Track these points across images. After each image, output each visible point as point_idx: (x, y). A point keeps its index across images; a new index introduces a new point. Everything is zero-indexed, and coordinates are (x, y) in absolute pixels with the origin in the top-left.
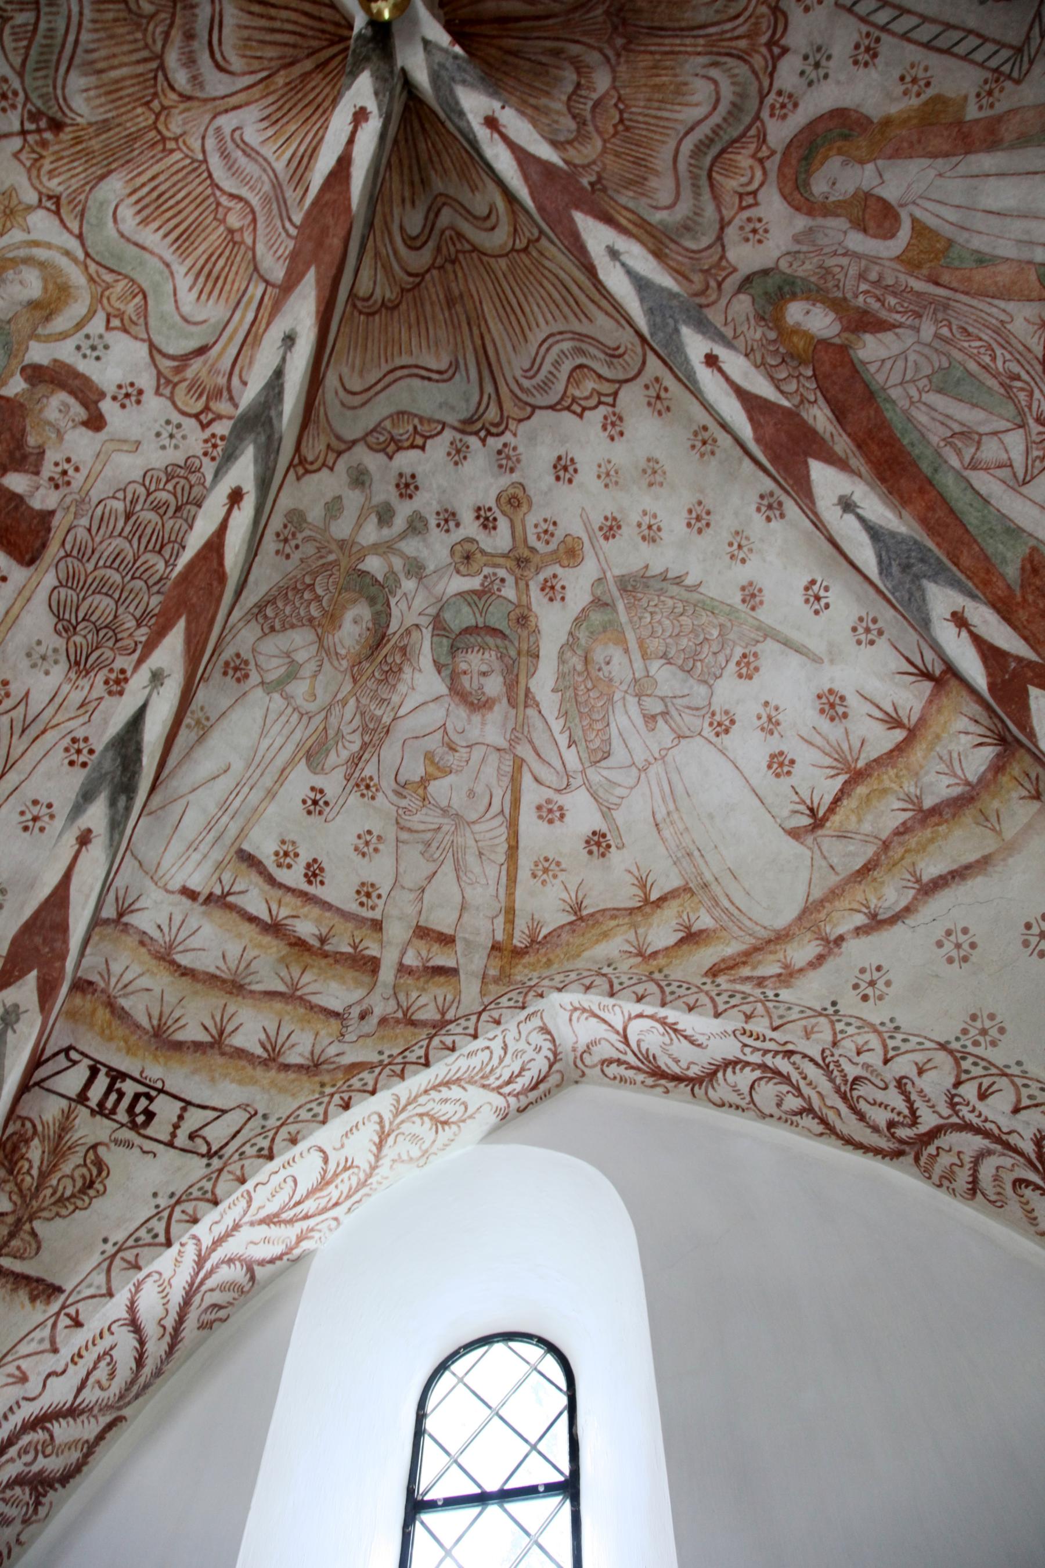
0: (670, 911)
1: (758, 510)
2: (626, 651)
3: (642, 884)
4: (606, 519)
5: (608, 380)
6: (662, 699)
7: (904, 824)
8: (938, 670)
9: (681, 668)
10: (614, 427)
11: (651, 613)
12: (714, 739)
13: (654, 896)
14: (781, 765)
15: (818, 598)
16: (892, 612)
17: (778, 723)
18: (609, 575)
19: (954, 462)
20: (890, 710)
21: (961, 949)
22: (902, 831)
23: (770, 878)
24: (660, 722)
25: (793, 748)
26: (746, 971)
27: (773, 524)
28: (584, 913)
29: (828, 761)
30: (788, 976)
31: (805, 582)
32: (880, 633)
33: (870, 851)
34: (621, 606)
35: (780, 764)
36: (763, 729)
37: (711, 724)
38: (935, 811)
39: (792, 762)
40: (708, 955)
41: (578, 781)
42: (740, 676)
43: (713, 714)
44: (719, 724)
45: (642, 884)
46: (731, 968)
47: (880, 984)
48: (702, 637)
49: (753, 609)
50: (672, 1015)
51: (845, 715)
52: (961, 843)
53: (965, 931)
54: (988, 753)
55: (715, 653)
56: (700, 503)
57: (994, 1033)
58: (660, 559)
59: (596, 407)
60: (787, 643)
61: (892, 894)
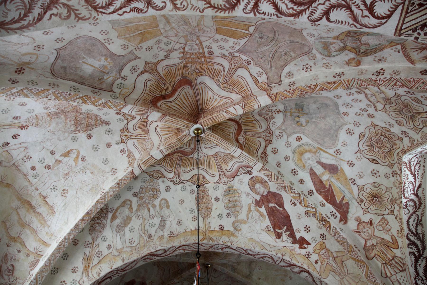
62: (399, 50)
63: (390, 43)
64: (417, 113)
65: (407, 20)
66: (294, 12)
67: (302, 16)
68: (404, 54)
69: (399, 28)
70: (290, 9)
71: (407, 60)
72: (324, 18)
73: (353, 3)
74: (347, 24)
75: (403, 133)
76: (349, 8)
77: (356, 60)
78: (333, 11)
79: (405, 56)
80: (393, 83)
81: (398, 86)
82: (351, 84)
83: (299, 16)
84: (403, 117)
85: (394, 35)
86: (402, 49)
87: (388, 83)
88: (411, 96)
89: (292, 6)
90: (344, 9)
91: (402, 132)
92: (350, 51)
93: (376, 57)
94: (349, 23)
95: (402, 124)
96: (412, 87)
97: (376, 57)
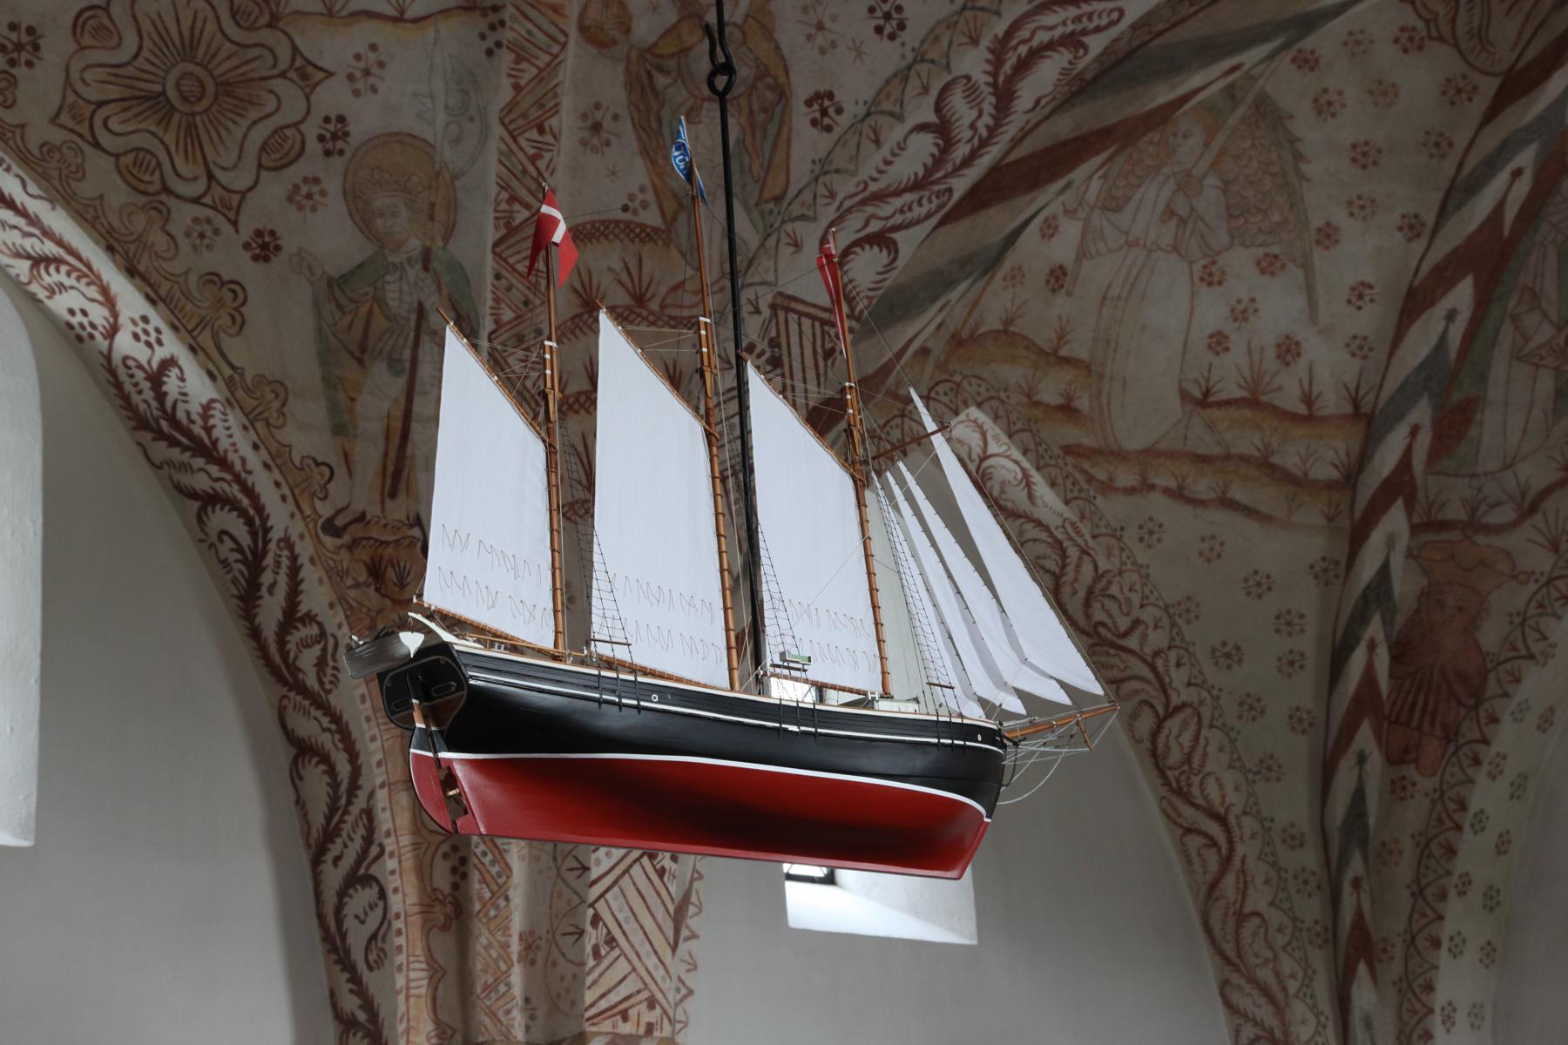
0: (1066, 375)
1: (1404, 216)
2: (1207, 145)
3: (1061, 336)
4: (1313, 52)
5: (1453, 29)
6: (1192, 209)
7: (1250, 457)
8: (1365, 409)
9: (1228, 207)
10: (1409, 42)
11: (1253, 145)
12: (1196, 279)
13: (1063, 352)
14: (1219, 343)
15: (1360, 297)
16: (1384, 358)
17: (1246, 320)
18: (1261, 82)
19: (1511, 304)
20: (1315, 393)
21: (1212, 552)
22: (1246, 459)
23: (1144, 412)
24: (1173, 223)
25: (1237, 342)
26: (1086, 465)
27: (1398, 236)
28: (1012, 329)
29: (1247, 374)
30: (1108, 488)
31: (1369, 279)
32: (1365, 357)
33: (1217, 451)
34: (1240, 112)
35: (1218, 342)
36: (1233, 310)
37: (1205, 267)
38: (1273, 468)
39: (1227, 349)
40: (1072, 434)
41: (1082, 214)
42: (1258, 264)
43: (1214, 263)
44: (1210, 274)
45: (1061, 336)
46: (1079, 455)
47: (1155, 537)
48: (1264, 207)
49: (1318, 242)
50: (1037, 478)
51: (1288, 364)
52: (1265, 496)
53: (1222, 544)
54: (1334, 474)
55: (1260, 230)
56: (1379, 151)
57: (1192, 615)
58: (1305, 127)
59: (1421, 17)
60: (1310, 288)
61: (1202, 486)
62: (635, 212)
63: (675, 196)
64: (191, 130)
65: (806, 323)
66: (1014, 43)
67: (988, 61)
68: (617, 223)
69: (794, 305)
70: (1033, 33)
71: (584, 225)
72: (931, 117)
73: (920, 200)
74: (875, 175)
75: (25, 38)
76: (917, 185)
77: (616, 33)
78: (937, 145)
79: (602, 222)
80: (523, 193)
81: (504, 206)
82: (533, 13)
83: (991, 51)
84: (145, 53)
85: (780, 294)
86: (643, 227)
87: (525, 171)
88: (311, 130)
89: (1035, 43)
90: (921, 174)
91: (31, 30)
92: (669, 31)
93: (616, 117)
94: (874, 180)
95: (87, 40)
96: (505, 260)
97: (616, 117)
